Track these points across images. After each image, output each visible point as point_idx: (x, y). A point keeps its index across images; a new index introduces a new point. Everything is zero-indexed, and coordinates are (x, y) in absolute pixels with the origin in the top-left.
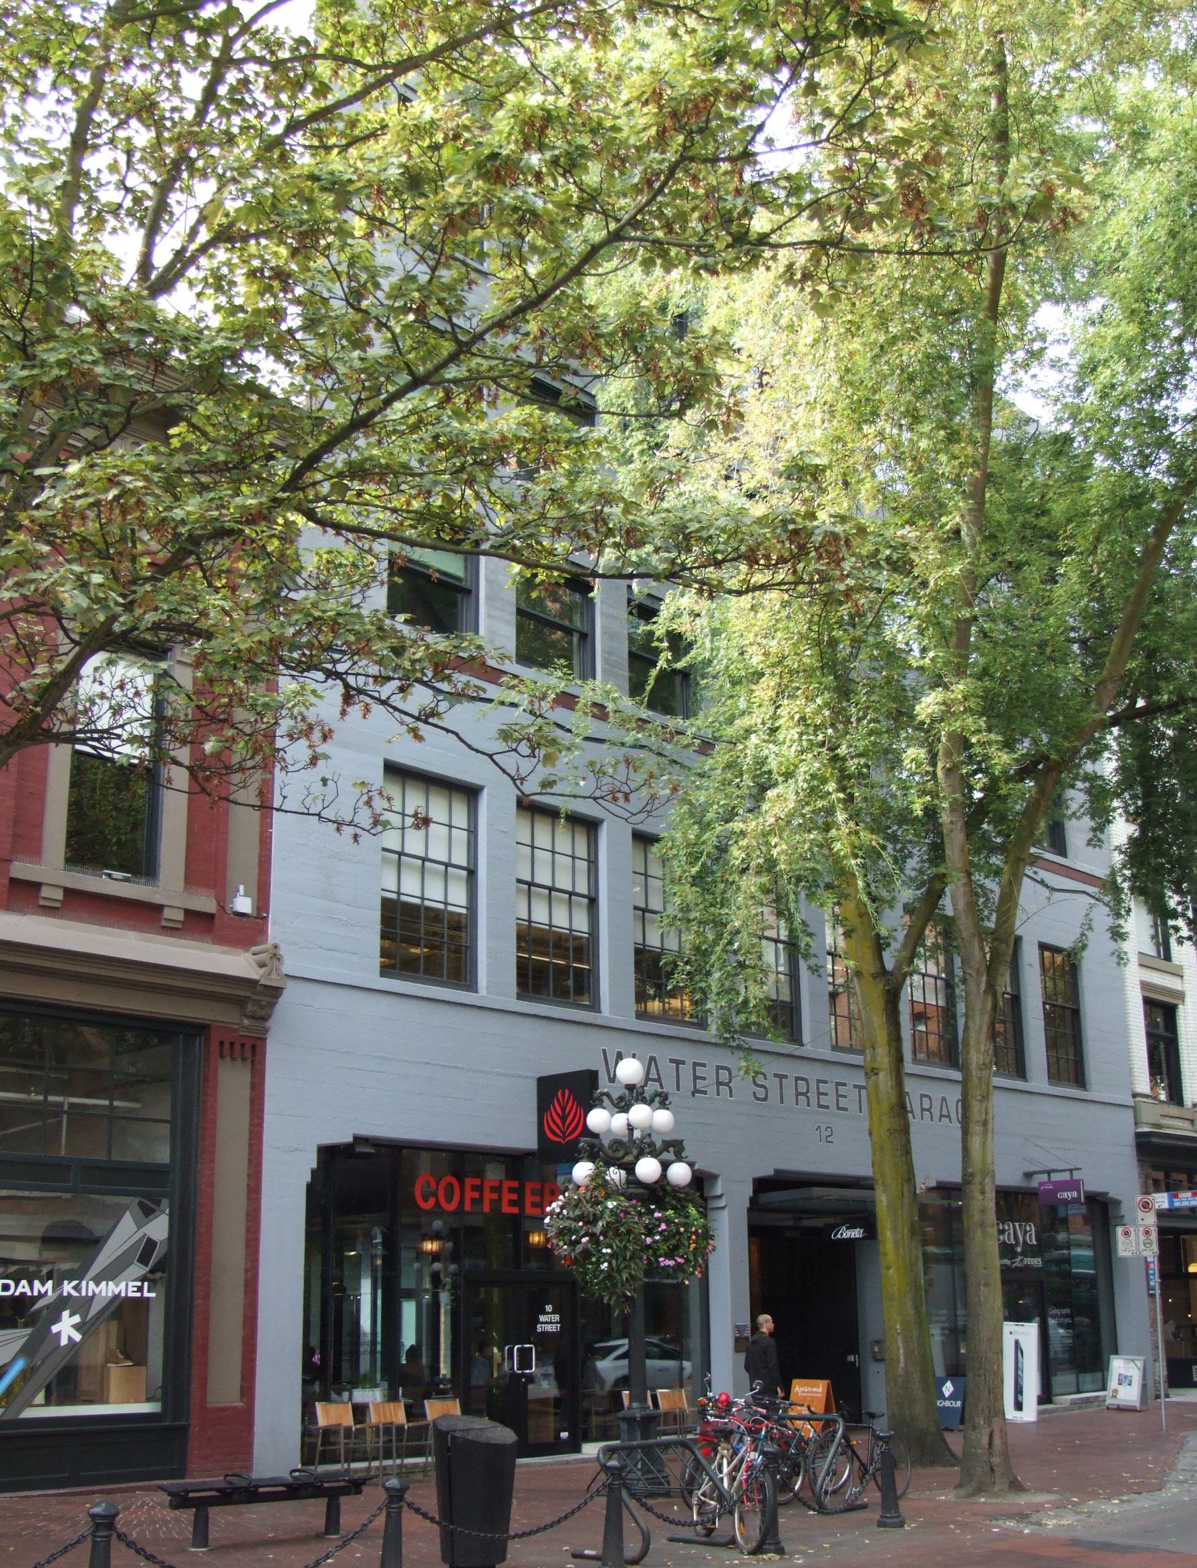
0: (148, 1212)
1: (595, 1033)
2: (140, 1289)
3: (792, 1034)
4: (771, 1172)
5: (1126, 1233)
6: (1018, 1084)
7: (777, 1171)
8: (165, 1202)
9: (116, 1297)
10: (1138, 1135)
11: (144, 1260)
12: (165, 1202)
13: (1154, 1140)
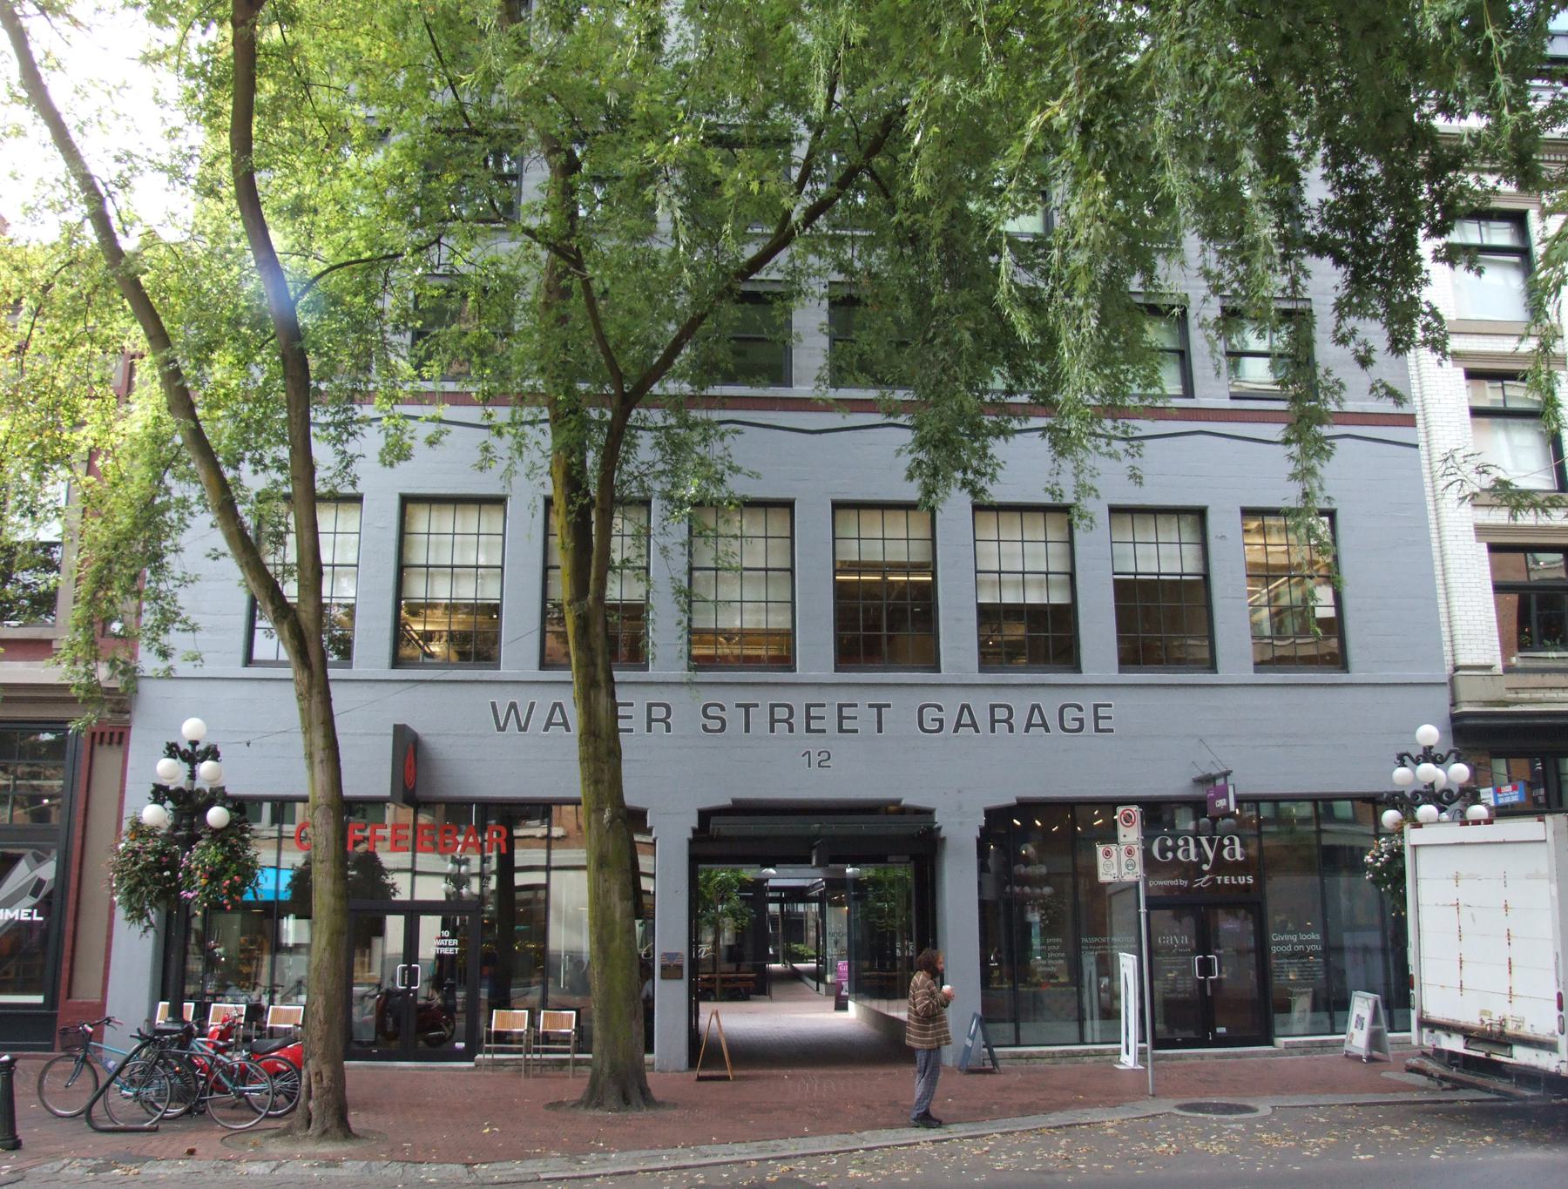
0: (40, 860)
1: (481, 688)
2: (31, 915)
3: (1263, 663)
4: (729, 802)
5: (1107, 854)
6: (1341, 678)
7: (734, 801)
8: (54, 853)
9: (11, 920)
10: (1455, 718)
11: (35, 893)
12: (54, 853)
13: (1467, 722)
